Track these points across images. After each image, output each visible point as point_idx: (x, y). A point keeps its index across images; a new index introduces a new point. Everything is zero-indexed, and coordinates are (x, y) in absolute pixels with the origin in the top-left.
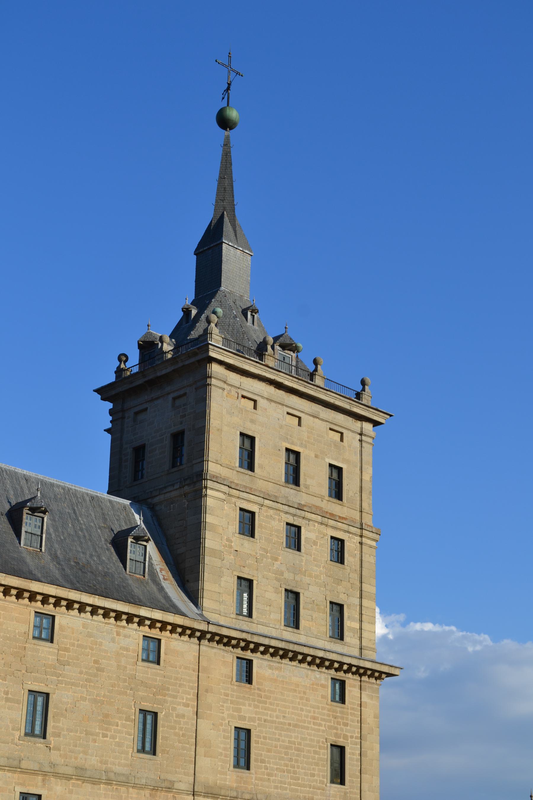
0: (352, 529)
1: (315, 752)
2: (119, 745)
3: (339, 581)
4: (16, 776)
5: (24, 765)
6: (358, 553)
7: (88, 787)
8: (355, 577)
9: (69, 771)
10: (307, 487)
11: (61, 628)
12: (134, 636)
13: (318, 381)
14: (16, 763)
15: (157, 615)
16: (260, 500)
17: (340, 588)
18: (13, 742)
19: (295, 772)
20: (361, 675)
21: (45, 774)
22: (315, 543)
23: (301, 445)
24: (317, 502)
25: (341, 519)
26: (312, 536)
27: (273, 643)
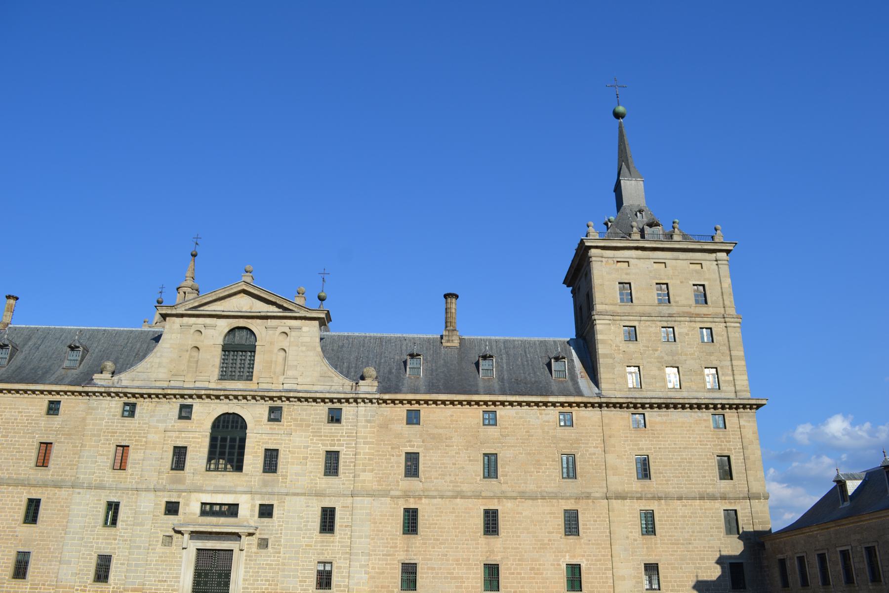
0: (716, 320)
1: (704, 462)
2: (548, 476)
3: (711, 354)
4: (480, 501)
5: (483, 494)
6: (725, 333)
7: (530, 502)
8: (725, 349)
9: (514, 494)
10: (676, 302)
11: (501, 417)
12: (553, 414)
15: (562, 399)
17: (712, 358)
19: (688, 477)
24: (687, 309)
25: (706, 315)
26: (684, 330)
27: (653, 401)
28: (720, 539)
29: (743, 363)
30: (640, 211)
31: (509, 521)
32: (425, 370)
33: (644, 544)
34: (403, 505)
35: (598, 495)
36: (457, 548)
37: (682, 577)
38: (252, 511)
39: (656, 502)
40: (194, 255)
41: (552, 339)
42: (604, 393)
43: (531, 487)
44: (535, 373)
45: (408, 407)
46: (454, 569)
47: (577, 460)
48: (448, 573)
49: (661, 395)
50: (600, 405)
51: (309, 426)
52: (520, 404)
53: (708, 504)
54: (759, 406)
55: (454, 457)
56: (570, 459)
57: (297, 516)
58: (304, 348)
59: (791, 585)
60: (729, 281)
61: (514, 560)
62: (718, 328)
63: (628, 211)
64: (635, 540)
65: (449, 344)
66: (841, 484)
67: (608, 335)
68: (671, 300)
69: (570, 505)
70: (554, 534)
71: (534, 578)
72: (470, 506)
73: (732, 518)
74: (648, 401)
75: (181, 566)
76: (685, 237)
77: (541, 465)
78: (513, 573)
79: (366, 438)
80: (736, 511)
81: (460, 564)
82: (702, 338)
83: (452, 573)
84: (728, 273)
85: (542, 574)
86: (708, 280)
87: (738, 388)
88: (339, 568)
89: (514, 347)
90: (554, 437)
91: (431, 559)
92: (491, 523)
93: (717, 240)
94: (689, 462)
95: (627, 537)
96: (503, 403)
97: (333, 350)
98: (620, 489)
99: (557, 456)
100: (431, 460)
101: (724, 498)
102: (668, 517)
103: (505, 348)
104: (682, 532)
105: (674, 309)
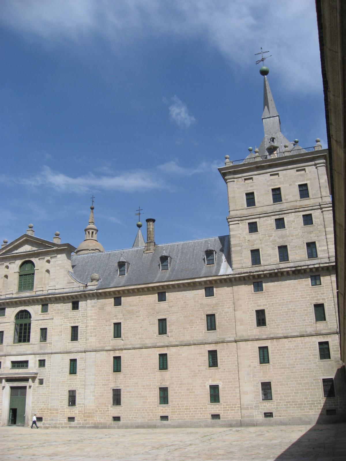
3: (311, 232)
17: (312, 235)
19: (293, 321)
22: (294, 221)
26: (292, 219)
28: (316, 363)
34: (113, 354)
38: (35, 363)
40: (92, 209)
46: (142, 392)
51: (62, 313)
57: (58, 365)
58: (58, 268)
62: (316, 215)
69: (212, 348)
70: (202, 367)
75: (2, 396)
78: (177, 393)
79: (91, 316)
81: (145, 389)
83: (141, 394)
85: (194, 392)
88: (79, 393)
94: (293, 311)
95: (250, 366)
97: (82, 266)
102: (278, 350)
104: (287, 360)
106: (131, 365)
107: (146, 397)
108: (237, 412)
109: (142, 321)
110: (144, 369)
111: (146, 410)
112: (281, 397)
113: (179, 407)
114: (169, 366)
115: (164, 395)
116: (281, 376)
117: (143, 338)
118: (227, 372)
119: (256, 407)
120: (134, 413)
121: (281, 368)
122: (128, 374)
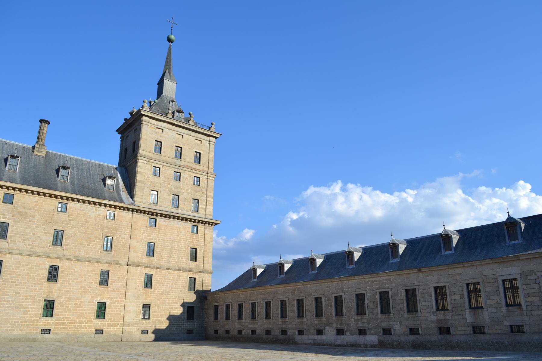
0: (203, 174)
2: (95, 248)
3: (197, 192)
4: (48, 259)
5: (51, 255)
6: (206, 182)
7: (81, 263)
9: (72, 257)
10: (184, 159)
11: (70, 207)
13: (191, 123)
14: (47, 255)
15: (111, 203)
16: (163, 163)
17: (197, 194)
18: (47, 247)
20: (205, 224)
21: (61, 259)
22: (187, 178)
23: (183, 145)
24: (189, 164)
25: (198, 170)
26: (186, 176)
27: (163, 213)
28: (185, 293)
29: (212, 200)
30: (173, 101)
31: (65, 274)
32: (20, 168)
33: (144, 293)
35: (122, 263)
36: (27, 288)
37: (162, 312)
39: (155, 270)
41: (106, 164)
42: (136, 203)
43: (83, 254)
44: (94, 184)
45: (6, 191)
46: (23, 302)
47: (114, 240)
48: (18, 305)
49: (167, 210)
50: (133, 210)
52: (84, 201)
53: (182, 273)
54: (216, 224)
55: (34, 229)
56: (110, 239)
59: (219, 318)
60: (213, 154)
61: (65, 298)
62: (203, 179)
63: (165, 99)
64: (140, 290)
65: (38, 154)
66: (254, 270)
67: (143, 170)
68: (182, 157)
69: (105, 267)
71: (76, 310)
72: (41, 262)
73: (193, 281)
74: (160, 212)
76: (196, 125)
77: (91, 241)
78: (63, 306)
80: (195, 278)
81: (28, 299)
82: (194, 181)
84: (213, 150)
86: (203, 151)
87: (207, 213)
89: (82, 164)
90: (102, 225)
91: (8, 295)
92: (53, 274)
93: (211, 130)
96: (73, 199)
98: (136, 260)
99: (102, 237)
100: (17, 229)
101: (190, 271)
103: (76, 164)
105: (182, 163)
106: (15, 272)
107: (28, 308)
108: (120, 329)
109: (36, 227)
110: (30, 278)
111: (26, 322)
112: (157, 317)
113: (64, 320)
114: (59, 279)
115: (49, 307)
116: (159, 300)
117: (34, 246)
118: (115, 291)
119: (135, 324)
120: (10, 324)
121: (160, 294)
122: (9, 282)
